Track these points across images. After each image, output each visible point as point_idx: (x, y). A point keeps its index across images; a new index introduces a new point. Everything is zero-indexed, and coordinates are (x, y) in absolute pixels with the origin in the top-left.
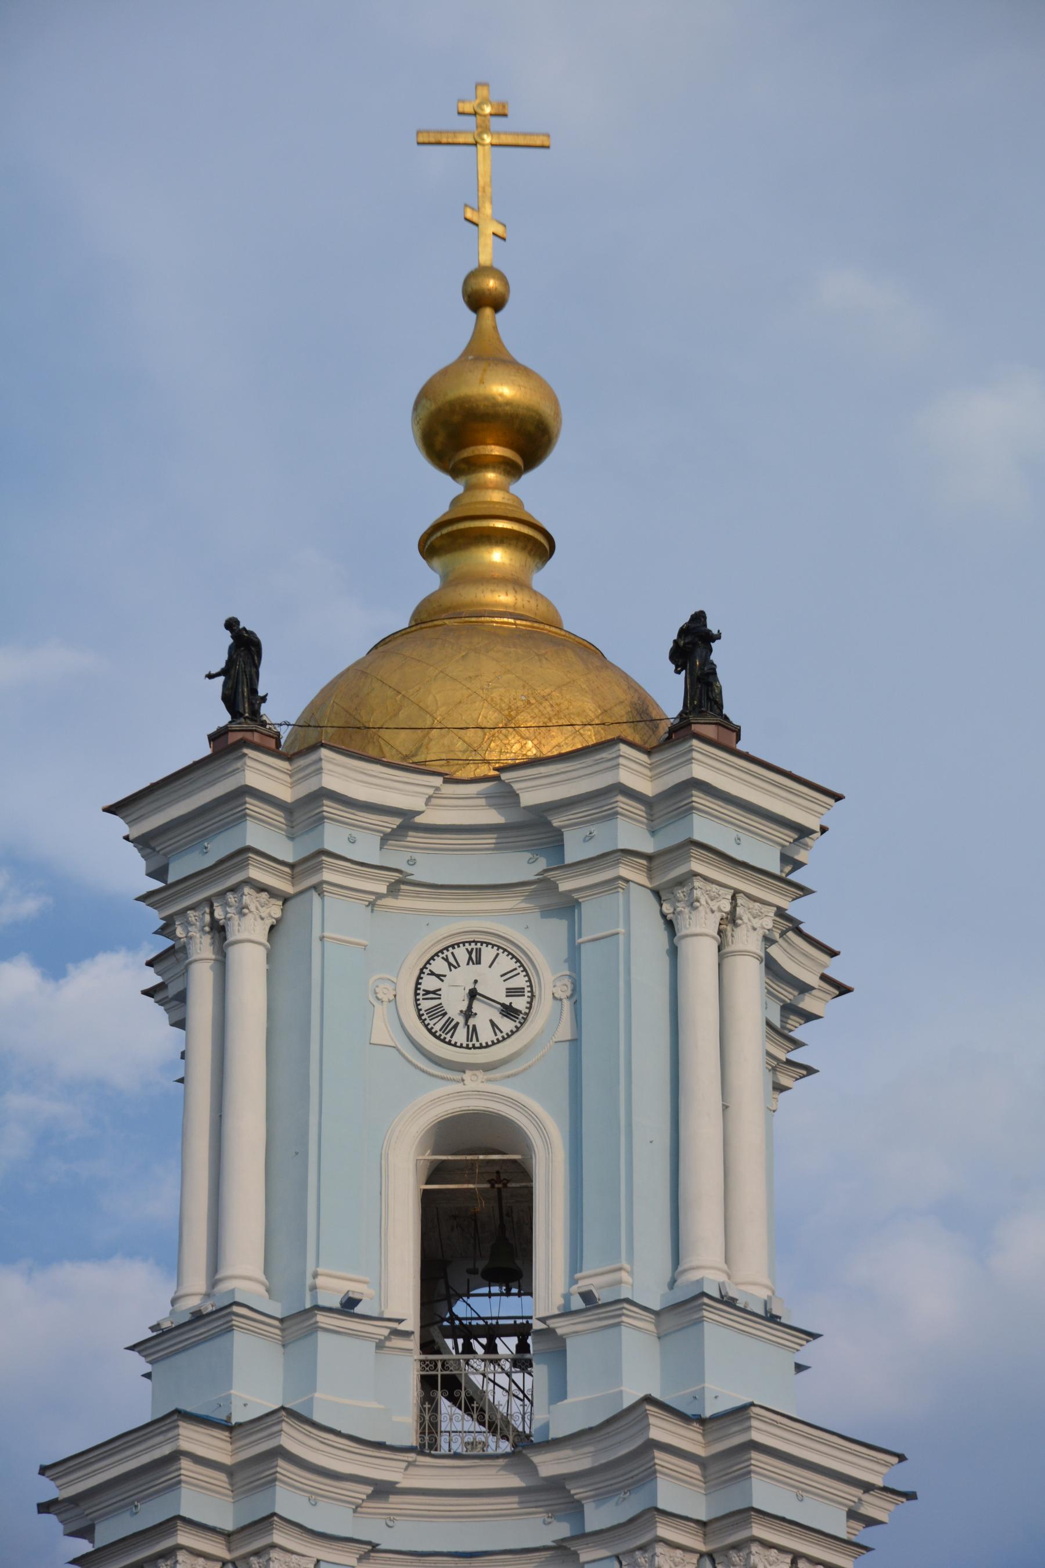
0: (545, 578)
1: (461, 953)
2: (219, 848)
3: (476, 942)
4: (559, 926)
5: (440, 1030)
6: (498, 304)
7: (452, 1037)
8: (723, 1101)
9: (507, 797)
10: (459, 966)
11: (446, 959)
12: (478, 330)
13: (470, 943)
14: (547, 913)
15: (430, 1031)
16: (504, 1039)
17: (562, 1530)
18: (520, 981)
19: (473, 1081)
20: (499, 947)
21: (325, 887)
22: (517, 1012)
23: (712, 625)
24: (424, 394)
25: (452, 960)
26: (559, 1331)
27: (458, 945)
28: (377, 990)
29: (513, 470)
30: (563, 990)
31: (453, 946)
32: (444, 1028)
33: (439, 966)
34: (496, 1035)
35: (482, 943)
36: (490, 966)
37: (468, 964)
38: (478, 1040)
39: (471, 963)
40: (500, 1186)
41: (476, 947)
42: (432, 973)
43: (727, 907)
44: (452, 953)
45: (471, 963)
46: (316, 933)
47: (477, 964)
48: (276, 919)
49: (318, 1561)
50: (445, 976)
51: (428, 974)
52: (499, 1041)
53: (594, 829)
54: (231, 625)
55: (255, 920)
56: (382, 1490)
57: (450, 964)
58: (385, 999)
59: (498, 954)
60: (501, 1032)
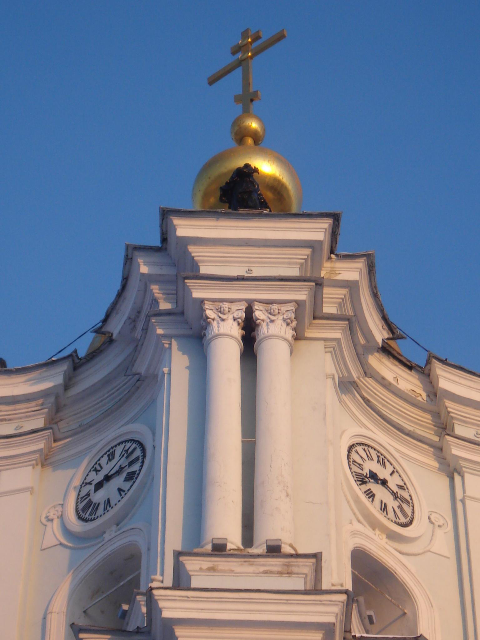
32: (91, 514)
42: (87, 484)
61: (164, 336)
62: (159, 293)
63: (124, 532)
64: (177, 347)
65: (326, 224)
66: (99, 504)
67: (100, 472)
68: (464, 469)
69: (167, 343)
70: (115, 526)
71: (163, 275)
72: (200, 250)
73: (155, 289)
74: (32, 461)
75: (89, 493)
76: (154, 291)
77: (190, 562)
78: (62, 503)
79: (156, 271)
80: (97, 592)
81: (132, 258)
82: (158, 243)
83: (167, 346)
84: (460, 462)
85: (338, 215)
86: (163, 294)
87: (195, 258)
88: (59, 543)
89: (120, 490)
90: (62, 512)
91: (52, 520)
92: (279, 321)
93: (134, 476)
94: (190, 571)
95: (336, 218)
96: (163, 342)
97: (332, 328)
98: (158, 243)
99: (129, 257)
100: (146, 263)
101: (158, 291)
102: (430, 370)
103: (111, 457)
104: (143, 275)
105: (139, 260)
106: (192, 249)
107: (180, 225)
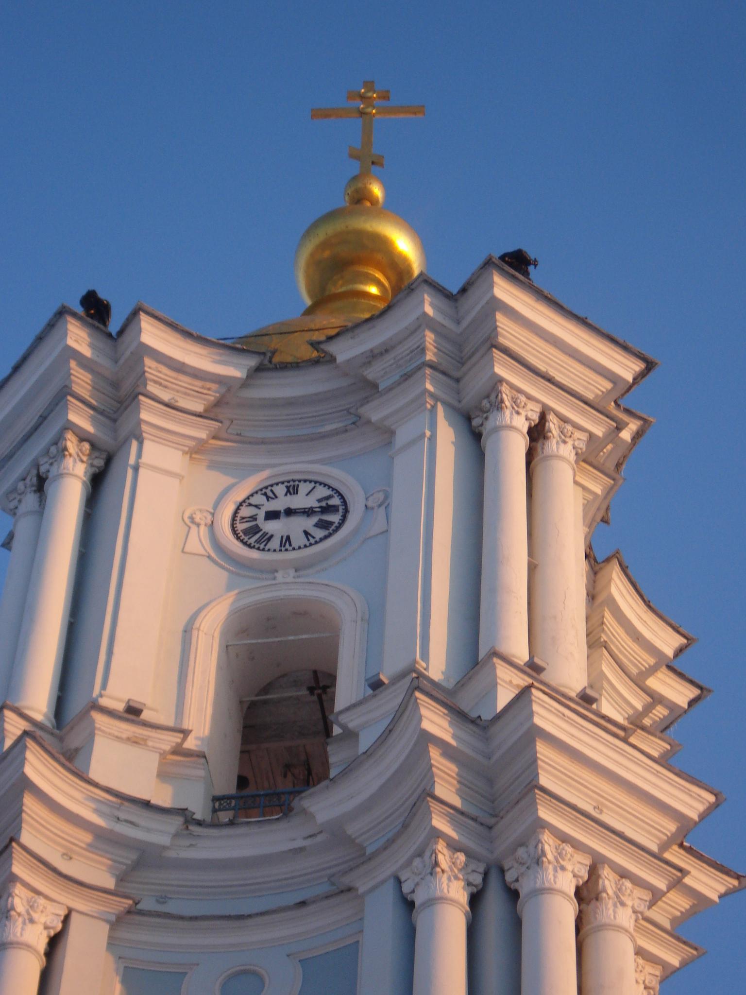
1: (280, 490)
3: (294, 481)
5: (255, 542)
7: (265, 545)
8: (529, 555)
10: (276, 497)
11: (265, 494)
13: (289, 482)
15: (245, 544)
16: (316, 543)
18: (336, 501)
20: (316, 482)
21: (144, 427)
22: (332, 523)
25: (270, 494)
26: (351, 725)
27: (277, 484)
28: (194, 516)
31: (272, 486)
32: (257, 541)
33: (259, 499)
34: (308, 540)
35: (300, 481)
36: (307, 495)
37: (286, 495)
38: (290, 545)
39: (288, 494)
40: (320, 691)
41: (294, 483)
42: (250, 505)
43: (535, 417)
44: (272, 491)
45: (288, 494)
46: (132, 460)
47: (294, 493)
48: (98, 467)
49: (70, 911)
50: (263, 505)
51: (247, 506)
52: (311, 545)
55: (75, 462)
57: (268, 498)
58: (203, 522)
59: (314, 488)
60: (314, 538)
61: (432, 395)
62: (430, 343)
63: (327, 585)
64: (443, 414)
65: (637, 366)
66: (272, 536)
67: (273, 500)
68: (604, 692)
69: (429, 403)
70: (294, 570)
71: (445, 327)
72: (508, 324)
73: (430, 337)
74: (185, 446)
75: (255, 517)
76: (428, 339)
77: (503, 668)
78: (212, 511)
79: (440, 318)
80: (243, 632)
81: (412, 290)
82: (455, 291)
83: (429, 406)
84: (604, 682)
85: (654, 364)
86: (435, 347)
87: (499, 329)
88: (208, 555)
89: (306, 533)
90: (212, 522)
91: (198, 525)
92: (569, 446)
93: (331, 527)
94: (500, 678)
95: (650, 366)
96: (428, 400)
97: (595, 479)
98: (455, 291)
99: (413, 286)
100: (431, 304)
101: (431, 341)
102: (601, 569)
103: (292, 490)
104: (425, 314)
105: (426, 296)
106: (499, 317)
107: (499, 285)
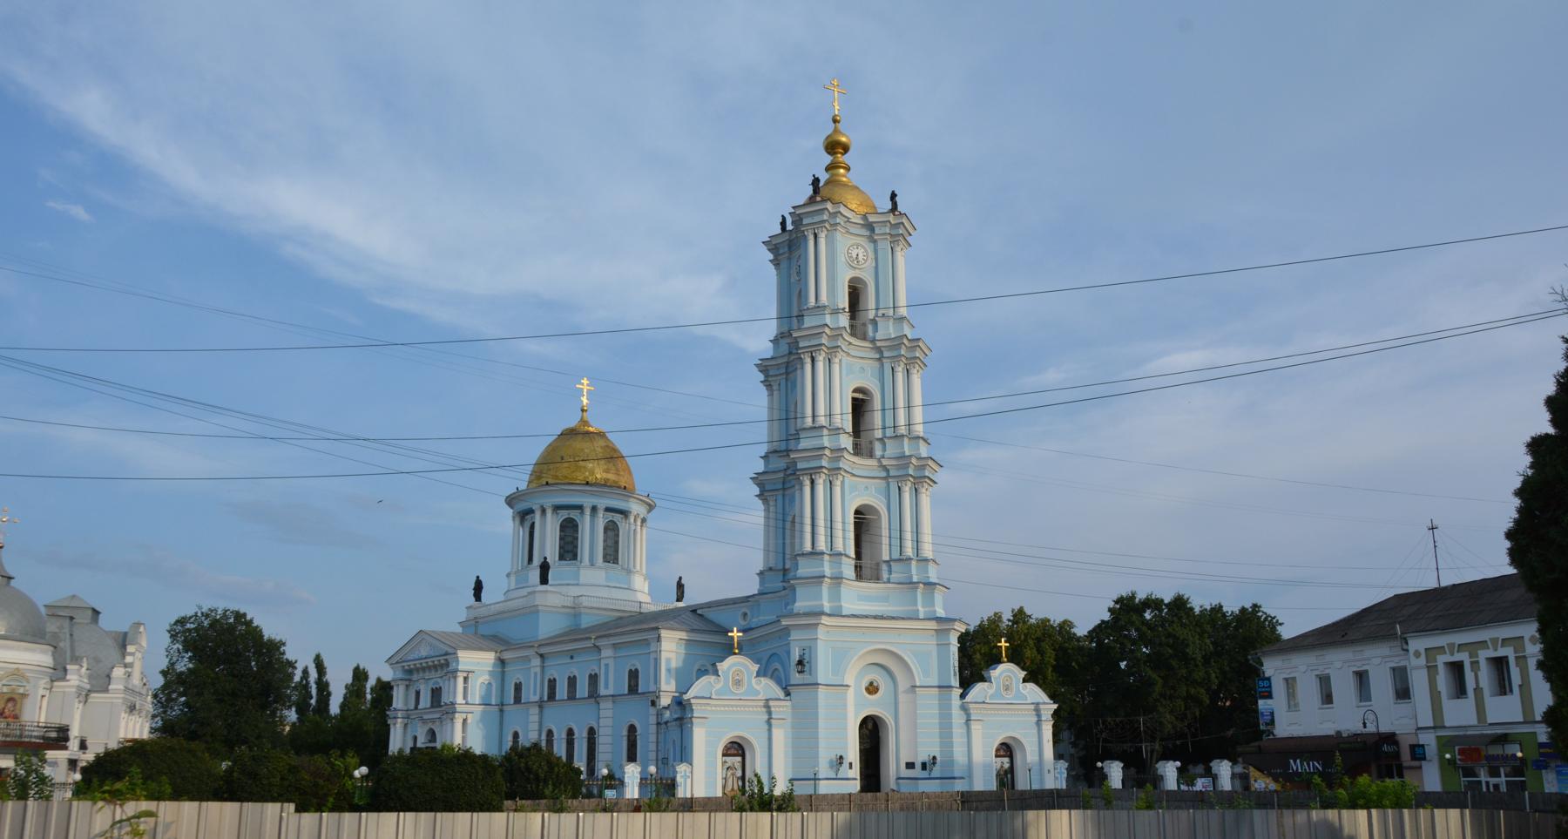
0: (849, 175)
1: (855, 247)
2: (817, 219)
4: (872, 245)
6: (839, 122)
9: (864, 217)
12: (835, 128)
14: (870, 242)
17: (877, 356)
19: (857, 271)
23: (896, 192)
24: (827, 138)
29: (843, 154)
30: (873, 257)
53: (883, 228)
54: (814, 176)
56: (850, 343)
